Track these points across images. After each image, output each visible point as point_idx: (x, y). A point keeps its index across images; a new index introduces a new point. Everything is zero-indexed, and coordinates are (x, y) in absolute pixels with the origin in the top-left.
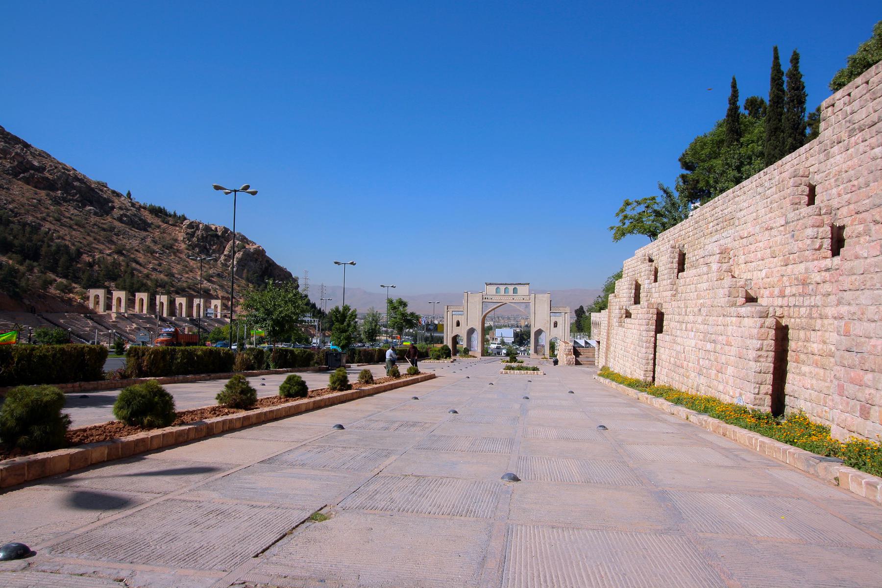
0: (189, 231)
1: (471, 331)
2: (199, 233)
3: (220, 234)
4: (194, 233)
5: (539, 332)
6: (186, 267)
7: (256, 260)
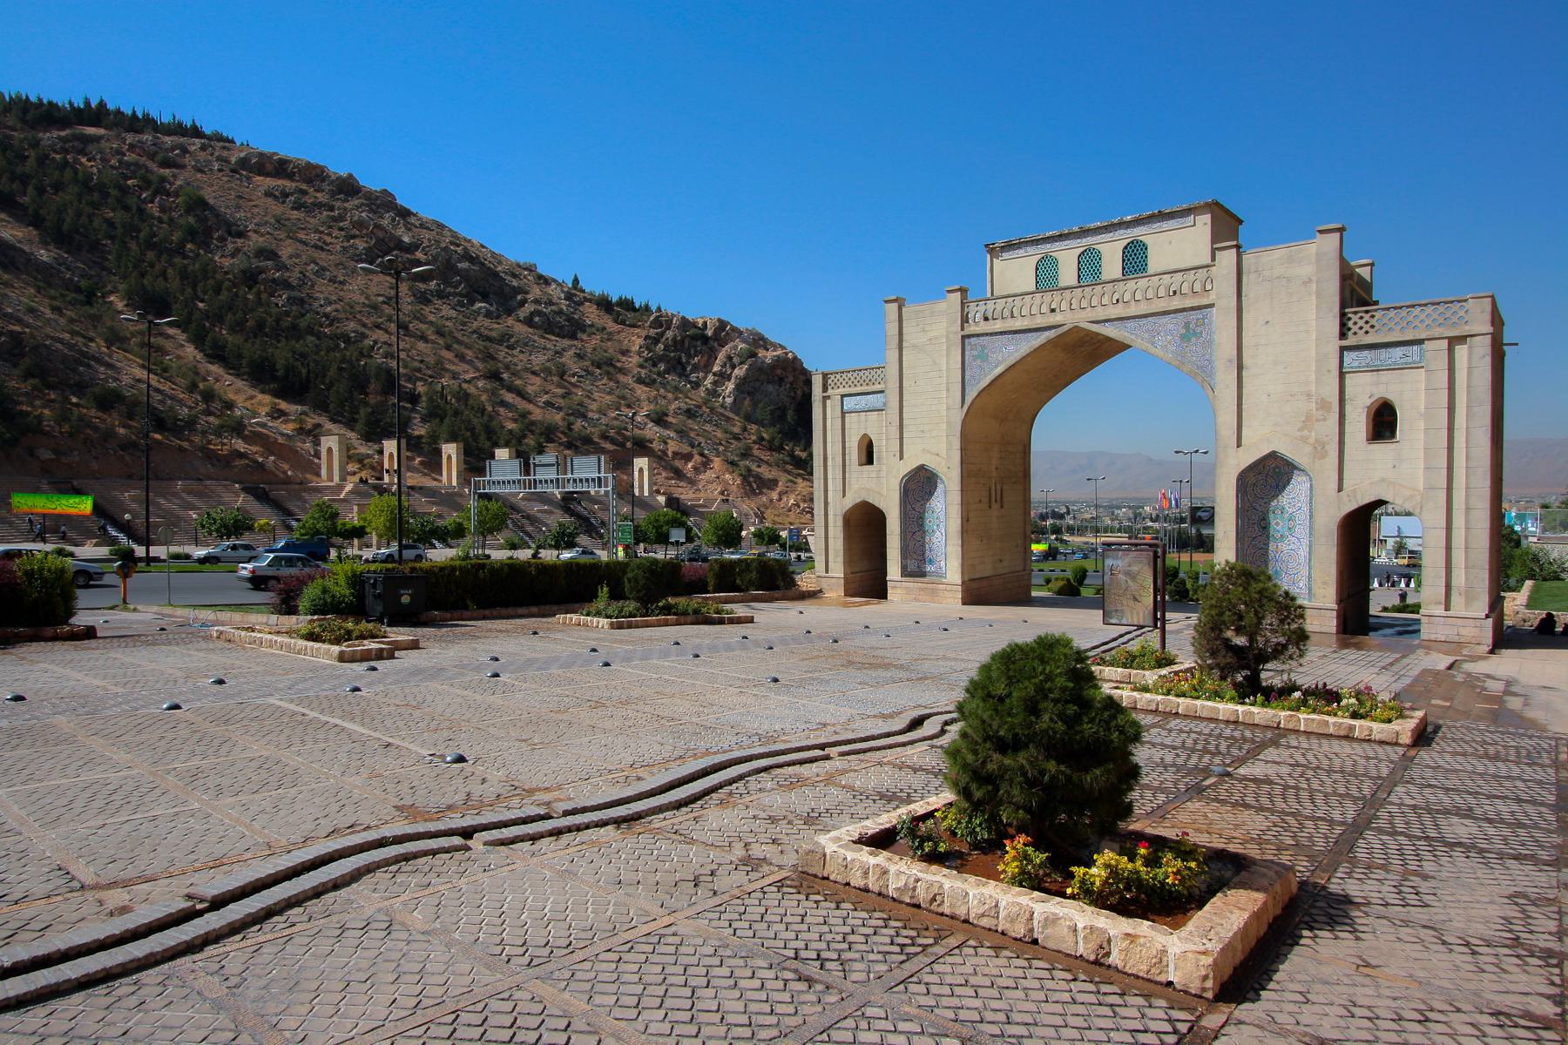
0: (653, 332)
1: (920, 485)
2: (669, 334)
3: (710, 333)
4: (662, 334)
5: (1267, 477)
6: (623, 398)
7: (781, 380)
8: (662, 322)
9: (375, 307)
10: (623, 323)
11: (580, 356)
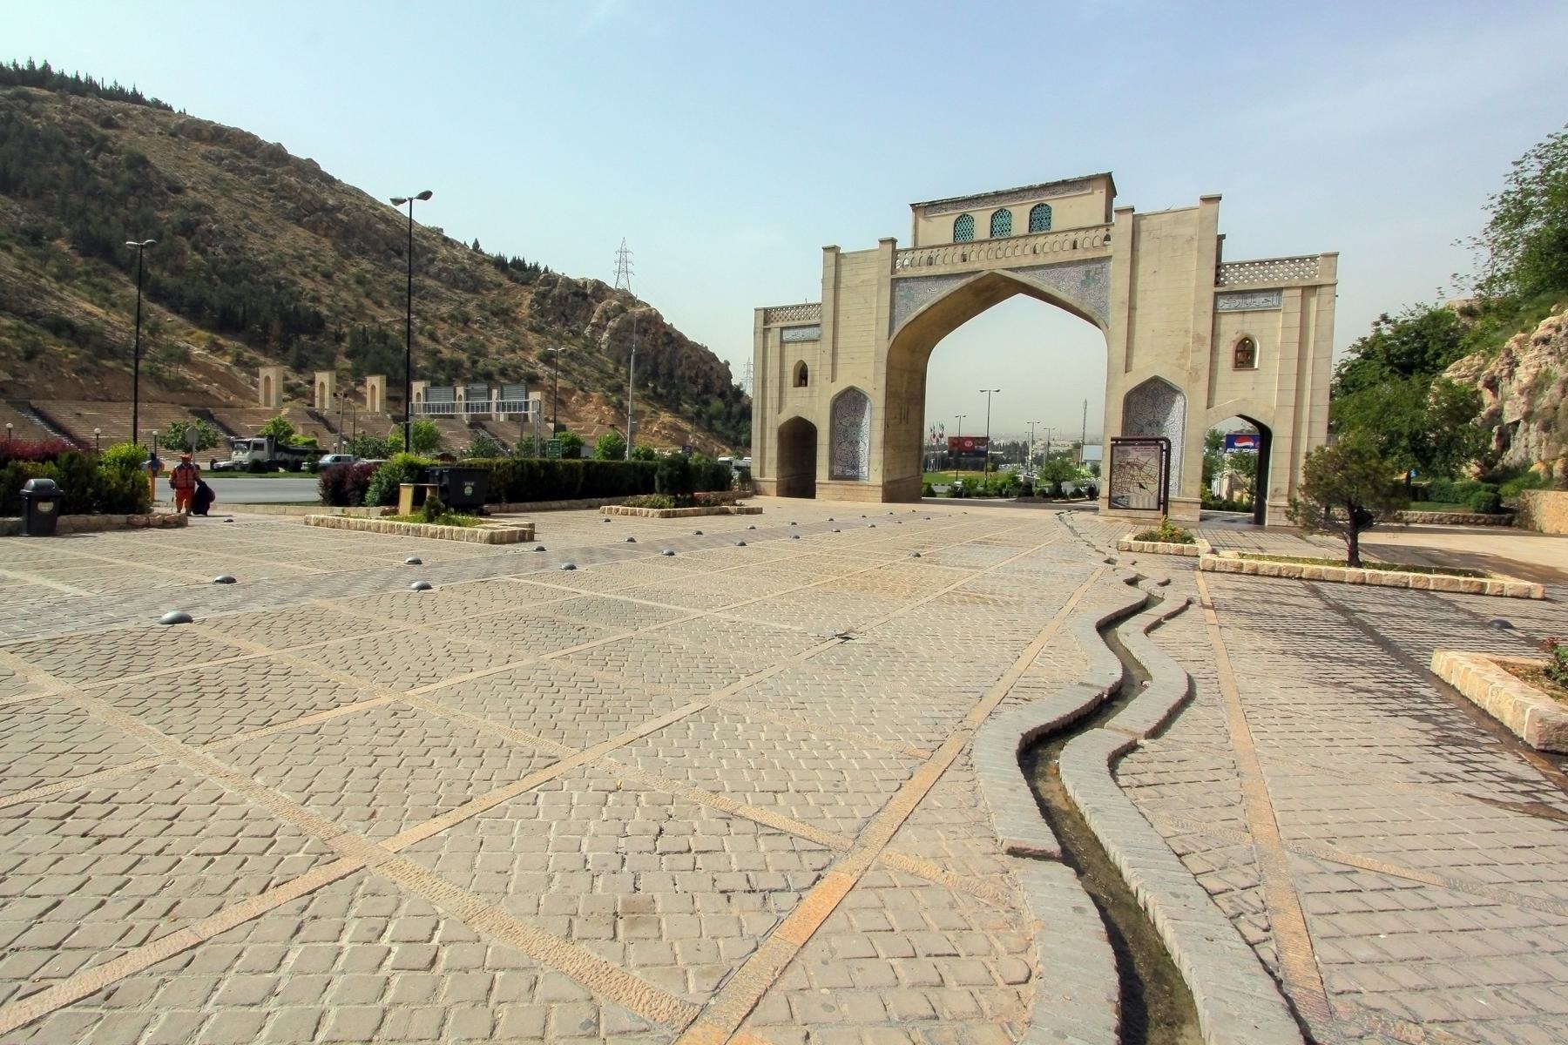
1: (849, 403)
2: (556, 291)
6: (517, 342)
8: (551, 280)
9: (301, 258)
10: (516, 281)
11: (481, 307)
